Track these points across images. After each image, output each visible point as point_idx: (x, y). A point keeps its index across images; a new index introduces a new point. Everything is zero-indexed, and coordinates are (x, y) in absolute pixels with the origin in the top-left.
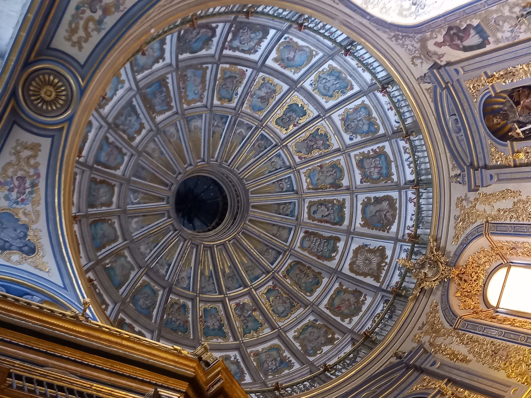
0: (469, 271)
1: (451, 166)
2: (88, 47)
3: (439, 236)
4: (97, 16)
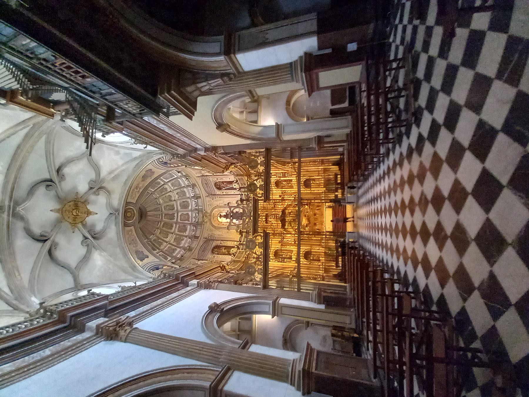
2: (136, 199)
4: (138, 190)
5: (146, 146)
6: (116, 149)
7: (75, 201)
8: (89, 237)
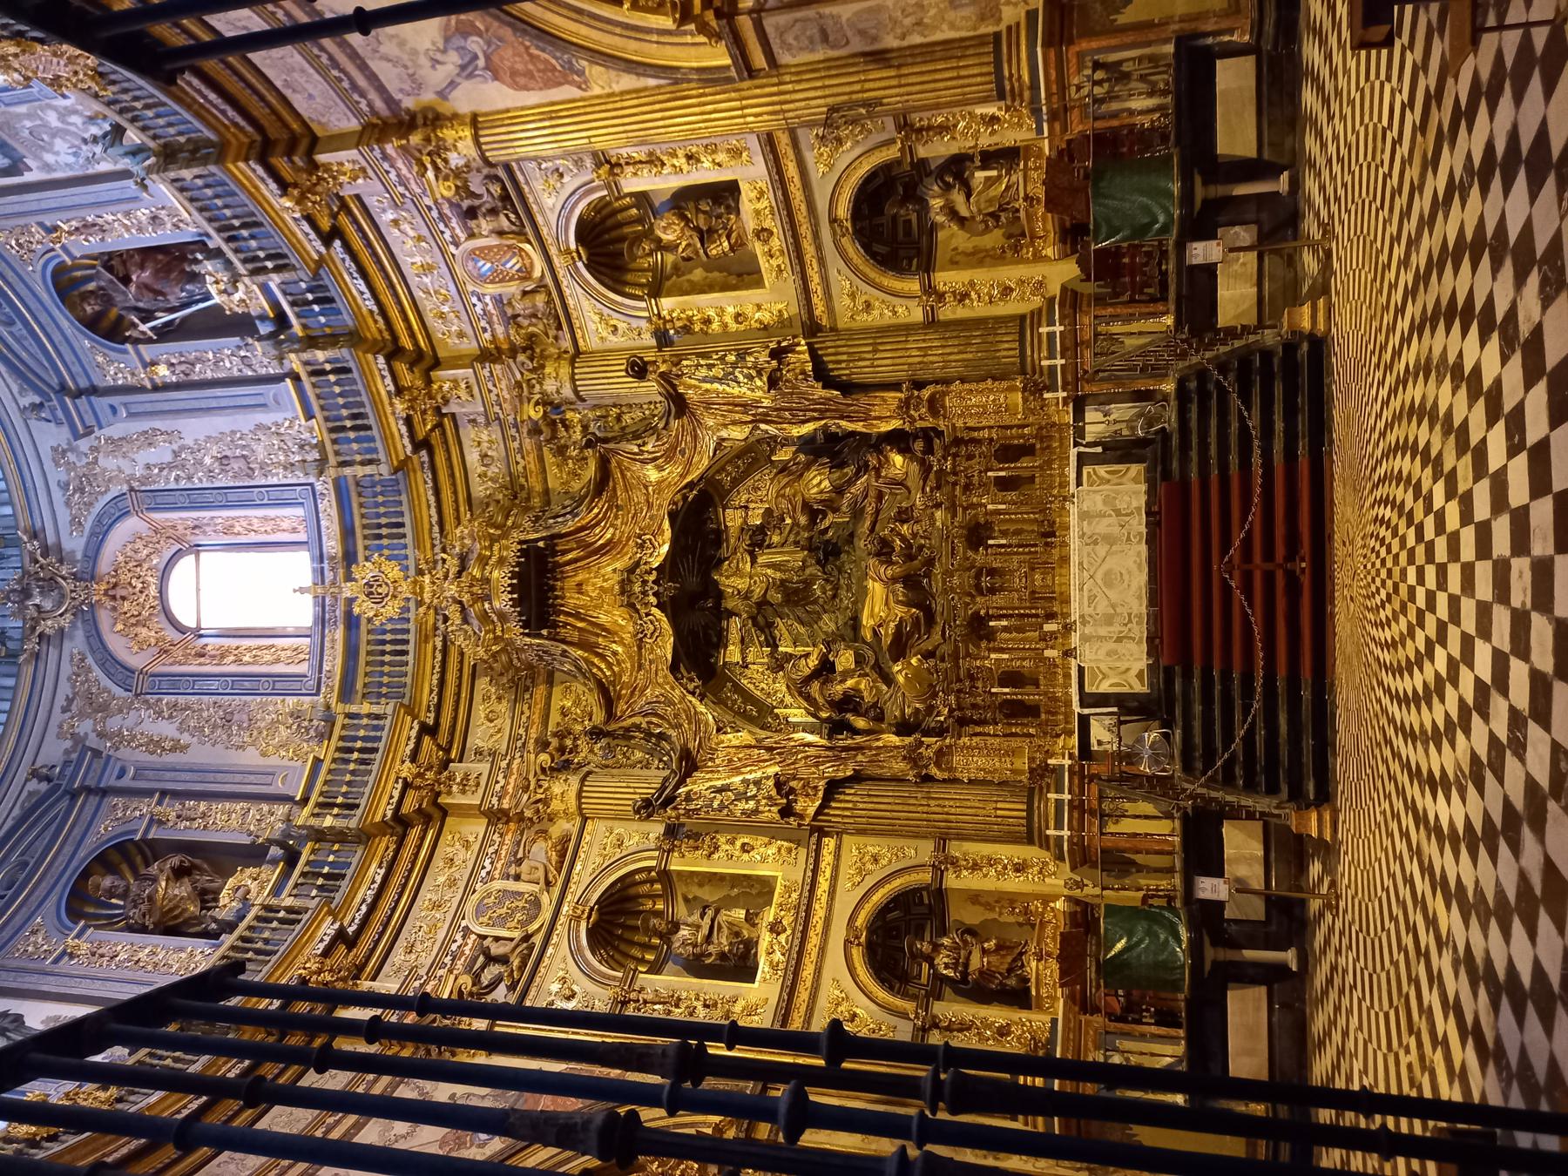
0: (124, 577)
1: (15, 389)
3: (38, 525)
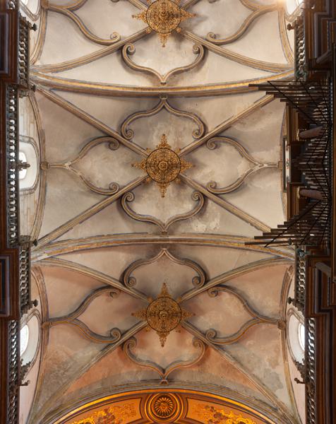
5: (301, 380)
6: (281, 359)
7: (181, 313)
8: (124, 338)
